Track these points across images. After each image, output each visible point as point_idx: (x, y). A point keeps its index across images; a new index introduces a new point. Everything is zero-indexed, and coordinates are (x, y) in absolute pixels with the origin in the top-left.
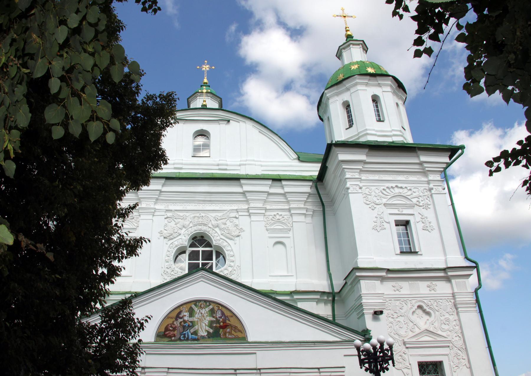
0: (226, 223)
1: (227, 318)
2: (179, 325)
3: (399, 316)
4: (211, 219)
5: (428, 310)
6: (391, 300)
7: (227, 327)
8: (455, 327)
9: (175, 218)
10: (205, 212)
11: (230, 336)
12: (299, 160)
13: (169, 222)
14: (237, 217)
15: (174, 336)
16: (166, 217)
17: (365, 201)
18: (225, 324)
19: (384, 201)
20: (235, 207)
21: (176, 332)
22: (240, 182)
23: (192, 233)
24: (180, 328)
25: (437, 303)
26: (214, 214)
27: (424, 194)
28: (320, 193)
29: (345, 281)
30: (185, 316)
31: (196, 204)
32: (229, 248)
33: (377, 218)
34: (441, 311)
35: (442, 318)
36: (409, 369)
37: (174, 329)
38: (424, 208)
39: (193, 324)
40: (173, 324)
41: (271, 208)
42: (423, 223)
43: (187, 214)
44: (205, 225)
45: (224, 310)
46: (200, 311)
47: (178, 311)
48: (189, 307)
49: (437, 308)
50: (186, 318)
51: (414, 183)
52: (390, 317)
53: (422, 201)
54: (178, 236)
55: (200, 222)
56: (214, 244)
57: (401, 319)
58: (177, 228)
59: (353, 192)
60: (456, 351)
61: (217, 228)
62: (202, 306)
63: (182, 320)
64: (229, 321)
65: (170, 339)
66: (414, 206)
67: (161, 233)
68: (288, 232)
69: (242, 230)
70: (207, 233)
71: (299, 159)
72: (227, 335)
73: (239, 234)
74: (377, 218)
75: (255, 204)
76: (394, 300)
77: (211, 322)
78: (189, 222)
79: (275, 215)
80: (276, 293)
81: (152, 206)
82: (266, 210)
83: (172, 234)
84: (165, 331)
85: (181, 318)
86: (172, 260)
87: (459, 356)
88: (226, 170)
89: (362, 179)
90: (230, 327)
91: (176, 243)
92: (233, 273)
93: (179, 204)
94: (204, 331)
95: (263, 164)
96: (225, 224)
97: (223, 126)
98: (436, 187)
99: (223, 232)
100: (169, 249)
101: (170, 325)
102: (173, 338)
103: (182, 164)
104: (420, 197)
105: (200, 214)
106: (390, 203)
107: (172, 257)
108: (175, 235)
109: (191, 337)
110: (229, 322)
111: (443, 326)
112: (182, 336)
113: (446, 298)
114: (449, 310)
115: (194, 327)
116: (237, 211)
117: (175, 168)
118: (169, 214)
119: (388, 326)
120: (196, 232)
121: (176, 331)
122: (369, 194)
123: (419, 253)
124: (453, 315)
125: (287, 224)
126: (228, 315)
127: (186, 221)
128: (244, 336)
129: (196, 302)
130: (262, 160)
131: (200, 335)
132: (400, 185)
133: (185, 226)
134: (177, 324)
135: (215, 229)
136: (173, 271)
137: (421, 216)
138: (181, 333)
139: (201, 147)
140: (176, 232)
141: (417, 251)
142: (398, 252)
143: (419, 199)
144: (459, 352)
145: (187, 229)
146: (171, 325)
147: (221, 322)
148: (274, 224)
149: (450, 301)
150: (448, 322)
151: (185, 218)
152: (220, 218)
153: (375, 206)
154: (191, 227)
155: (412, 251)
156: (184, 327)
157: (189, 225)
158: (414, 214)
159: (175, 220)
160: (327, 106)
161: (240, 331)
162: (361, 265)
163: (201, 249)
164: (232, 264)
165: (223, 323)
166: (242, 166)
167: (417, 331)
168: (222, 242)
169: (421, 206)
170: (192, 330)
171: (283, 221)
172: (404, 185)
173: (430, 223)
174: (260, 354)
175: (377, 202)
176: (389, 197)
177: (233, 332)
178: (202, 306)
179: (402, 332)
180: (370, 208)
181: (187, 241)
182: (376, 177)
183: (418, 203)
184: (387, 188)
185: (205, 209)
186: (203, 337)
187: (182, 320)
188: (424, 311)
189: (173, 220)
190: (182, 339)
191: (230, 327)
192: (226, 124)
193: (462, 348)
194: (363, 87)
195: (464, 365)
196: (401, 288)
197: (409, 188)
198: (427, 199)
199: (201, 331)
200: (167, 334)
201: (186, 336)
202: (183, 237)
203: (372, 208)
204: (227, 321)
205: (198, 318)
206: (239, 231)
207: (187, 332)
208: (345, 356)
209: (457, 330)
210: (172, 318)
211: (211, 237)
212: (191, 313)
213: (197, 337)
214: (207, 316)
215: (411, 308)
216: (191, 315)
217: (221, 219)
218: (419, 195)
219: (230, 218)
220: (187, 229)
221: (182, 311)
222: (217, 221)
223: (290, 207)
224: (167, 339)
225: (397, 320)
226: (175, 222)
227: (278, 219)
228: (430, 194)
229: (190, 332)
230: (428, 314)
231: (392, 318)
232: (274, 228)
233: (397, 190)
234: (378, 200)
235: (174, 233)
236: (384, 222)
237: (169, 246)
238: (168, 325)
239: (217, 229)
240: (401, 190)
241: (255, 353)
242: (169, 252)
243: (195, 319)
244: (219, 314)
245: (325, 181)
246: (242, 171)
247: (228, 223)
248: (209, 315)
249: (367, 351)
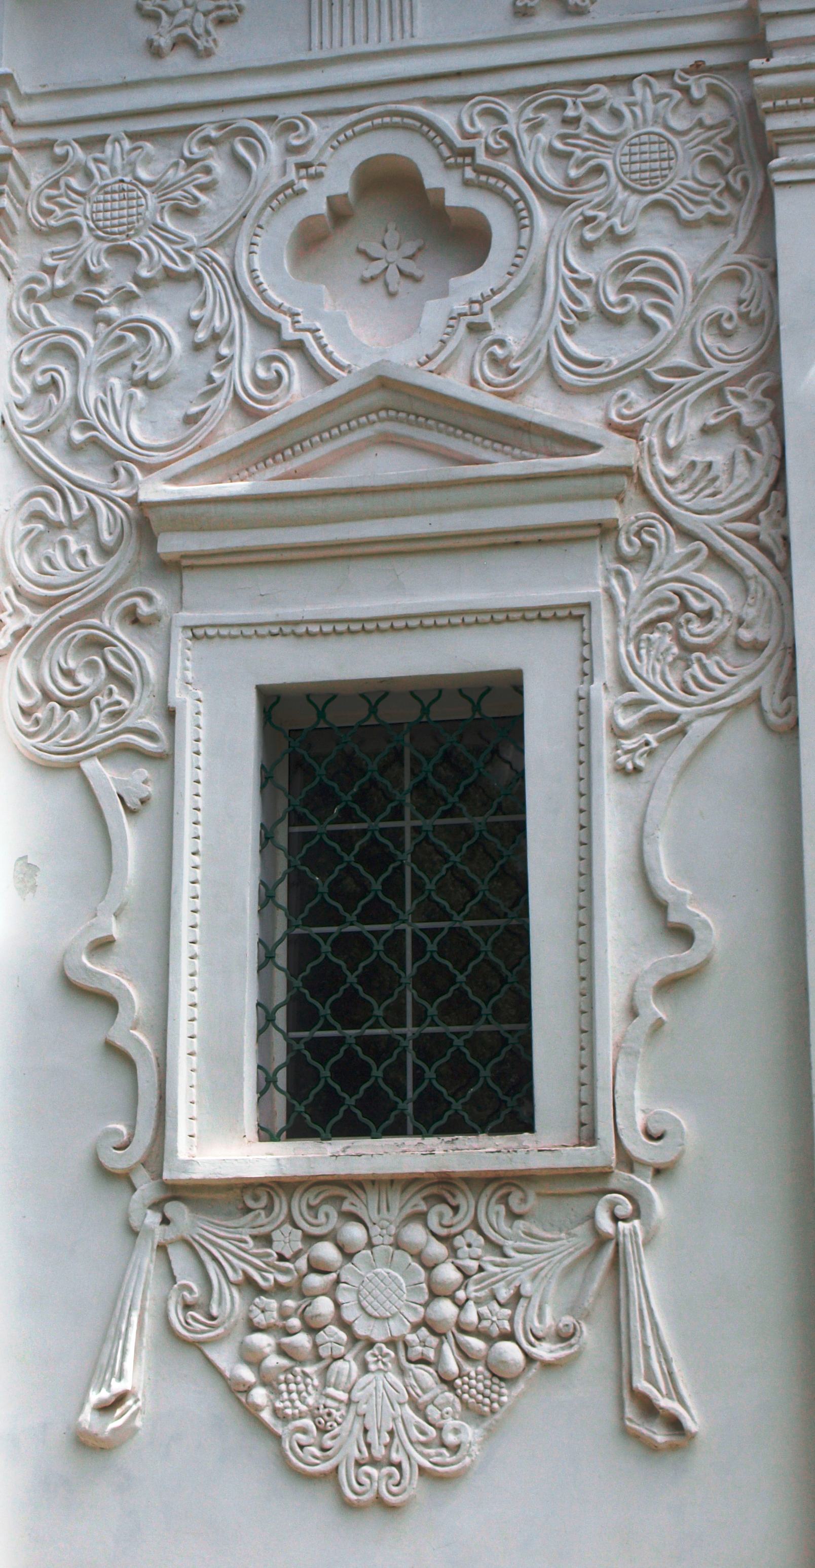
25: (566, 121)
60: (683, 571)
76: (133, 136)
113: (687, 60)
195: (737, 708)
196: (221, 22)
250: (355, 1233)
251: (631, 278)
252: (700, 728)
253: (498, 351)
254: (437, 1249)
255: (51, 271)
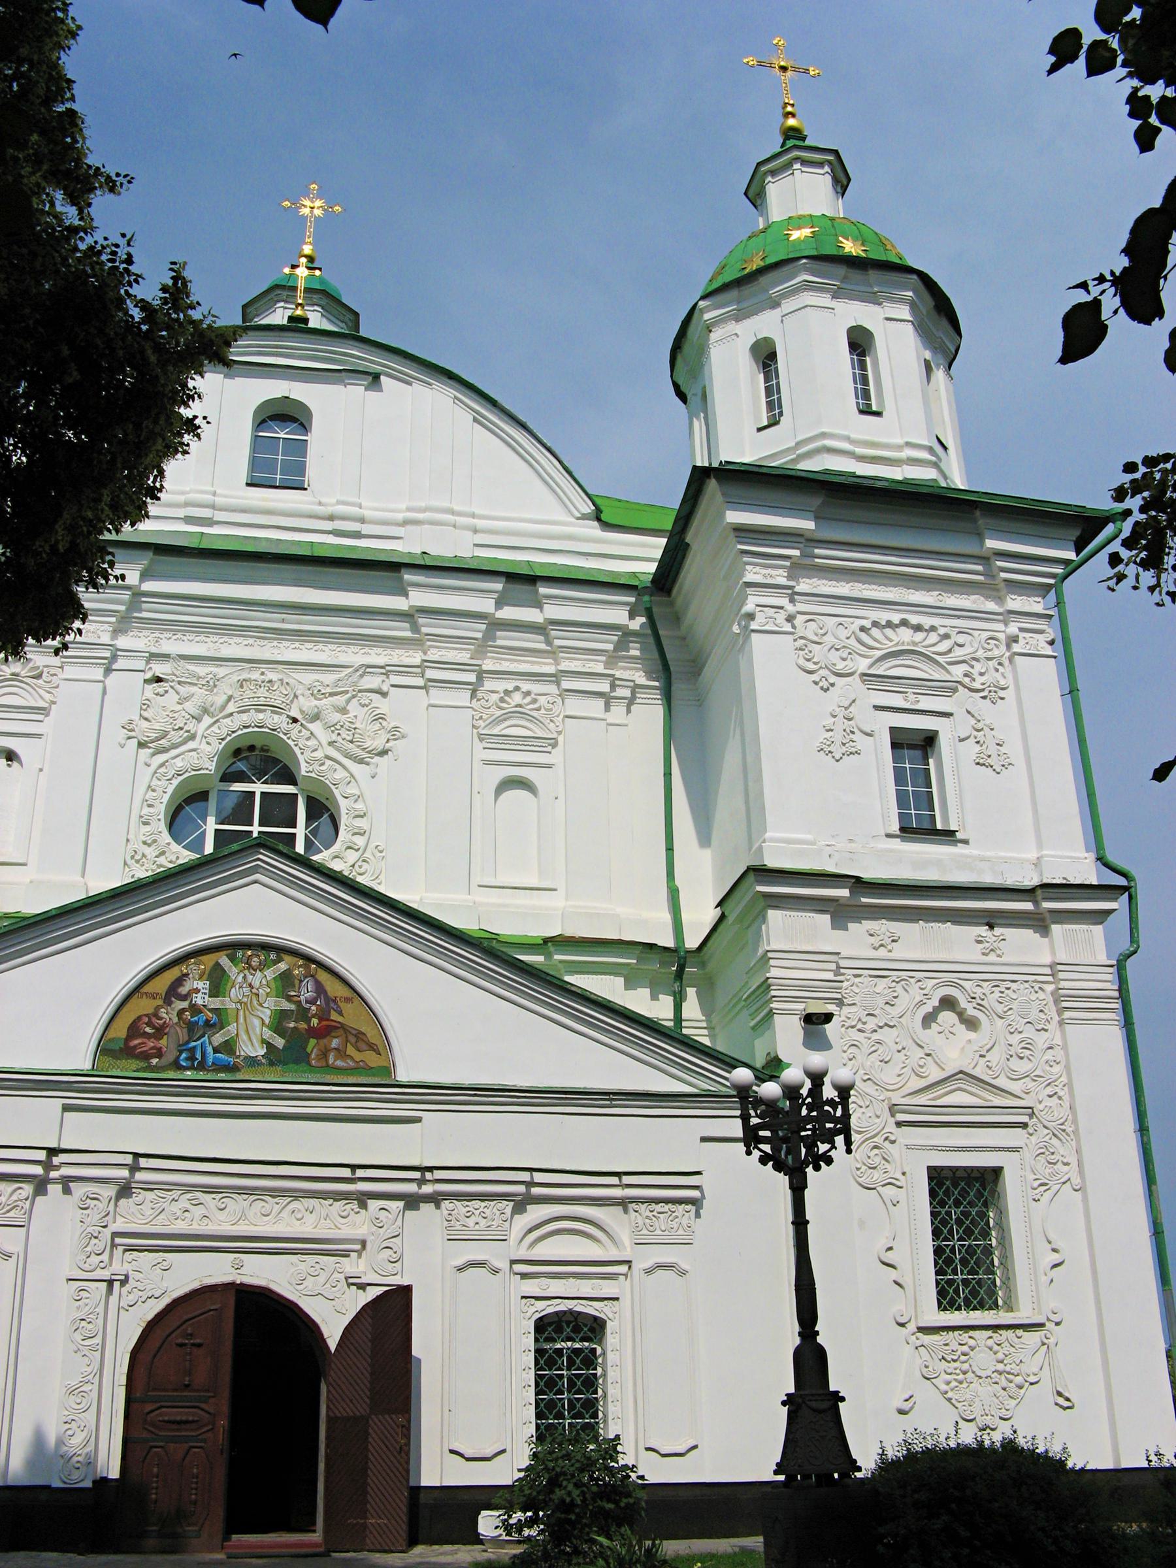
0: (348, 708)
1: (332, 1005)
2: (176, 1020)
3: (881, 1027)
4: (298, 693)
5: (971, 1011)
6: (860, 976)
7: (333, 1034)
8: (1048, 1068)
9: (180, 683)
10: (280, 667)
11: (339, 1063)
12: (598, 519)
13: (157, 694)
14: (385, 688)
15: (159, 1053)
16: (149, 675)
17: (801, 662)
18: (324, 1023)
19: (863, 665)
20: (378, 656)
21: (163, 1042)
22: (401, 579)
23: (234, 735)
24: (177, 1028)
26: (308, 677)
27: (989, 654)
28: (661, 632)
29: (718, 911)
30: (197, 991)
31: (251, 641)
32: (352, 790)
33: (835, 716)
34: (1012, 1017)
35: (1016, 1038)
36: (901, 1187)
37: (160, 1032)
38: (984, 698)
39: (219, 1020)
40: (156, 1015)
41: (498, 668)
42: (978, 742)
43: (221, 671)
44: (276, 709)
45: (323, 976)
46: (245, 977)
47: (174, 973)
48: (214, 962)
49: (1000, 1009)
50: (199, 999)
51: (959, 617)
52: (853, 1027)
53: (982, 674)
54: (184, 742)
55: (262, 701)
56: (303, 773)
57: (886, 1035)
58: (183, 713)
59: (766, 628)
60: (1047, 1139)
61: (318, 722)
62: (255, 962)
63: (185, 1004)
64: (340, 1013)
65: (144, 1064)
66: (955, 690)
67: (128, 727)
68: (549, 749)
69: (396, 734)
70: (281, 735)
71: (598, 516)
72: (331, 1061)
73: (388, 745)
74: (835, 716)
75: (443, 652)
76: (871, 976)
77: (282, 1015)
78: (225, 698)
79: (507, 692)
80: (495, 937)
81: (106, 639)
82: (481, 675)
83: (165, 734)
84: (129, 1037)
85: (184, 998)
86: (162, 816)
87: (1053, 1153)
88: (357, 535)
89: (796, 590)
90: (341, 1032)
91: (179, 763)
92: (362, 871)
93: (192, 636)
94: (257, 1043)
95: (481, 523)
96: (343, 711)
97: (356, 391)
98: (1027, 635)
99: (334, 737)
100: (155, 782)
101: (146, 1020)
102: (155, 1061)
103: (213, 507)
104: (974, 663)
105: (263, 674)
106: (880, 672)
107: (163, 807)
108: (175, 737)
109: (215, 1058)
110: (340, 1019)
111: (1015, 1064)
112: (184, 1055)
114: (1034, 1015)
115: (222, 1028)
116: (386, 670)
117: (189, 520)
118: (159, 669)
119: (845, 1055)
120: (245, 731)
121: (165, 1037)
122: (815, 639)
123: (959, 835)
124: (1046, 1030)
125: (547, 722)
126: (339, 994)
127: (216, 694)
128: (385, 1064)
129: (233, 947)
130: (478, 512)
131: (242, 1053)
132: (914, 619)
133: (212, 709)
134: (169, 1015)
135: (310, 726)
136: (163, 853)
137: (973, 721)
138: (180, 1045)
139: (280, 457)
140: (181, 729)
141: (952, 829)
142: (895, 828)
143: (972, 667)
144: (1055, 1141)
145: (217, 721)
146: (149, 1019)
147: (314, 1016)
148: (505, 720)
149: (1040, 988)
150: (1028, 1052)
151: (211, 683)
152: (329, 690)
153: (833, 679)
154: (231, 714)
155: (939, 827)
156: (191, 1027)
157: (223, 707)
158: (951, 714)
159: (178, 687)
160: (703, 350)
161: (372, 1047)
162: (772, 862)
163: (258, 788)
164: (360, 841)
165: (321, 1019)
166: (409, 528)
167: (935, 1075)
168: (331, 767)
169: (977, 691)
170: (218, 1039)
171: (534, 714)
172: (927, 621)
173: (1001, 746)
174: (433, 1120)
175: (840, 666)
176: (879, 653)
177: (351, 1050)
178: (253, 964)
179: (888, 1076)
180: (816, 683)
181: (215, 759)
182: (844, 588)
183: (967, 680)
184: (875, 624)
185: (280, 658)
186: (252, 1061)
187: (185, 1004)
188: (961, 1015)
189: (172, 687)
190: (184, 1064)
191: (341, 1032)
192: (366, 389)
193: (1064, 1131)
194: (825, 300)
196: (893, 941)
197: (942, 631)
198: (997, 670)
199: (249, 1044)
200: (135, 1047)
201: (199, 1056)
202: (204, 746)
203: (821, 684)
204: (332, 1012)
205: (240, 1002)
206: (389, 736)
207: (199, 1042)
208: (704, 1139)
209: (1054, 1077)
210: (153, 996)
211: (296, 750)
212: (218, 982)
213: (231, 1060)
214: (268, 994)
215: (921, 1003)
216: (215, 992)
217: (331, 695)
218: (973, 656)
219: (360, 691)
220: (217, 721)
221: (187, 975)
222: (320, 699)
223: (560, 668)
224: (134, 1064)
225: (875, 1036)
226: (178, 693)
227: (516, 706)
228: (1007, 654)
229: (210, 1043)
230: (971, 1024)
231: (859, 1030)
232: (504, 732)
233: (905, 636)
234: (844, 660)
235: (174, 730)
236: (855, 730)
237: (155, 772)
238: (139, 1018)
239: (316, 727)
240: (920, 636)
241: (418, 1120)
242: (154, 791)
243: (227, 1003)
244: (306, 992)
245: (679, 592)
246: (407, 545)
247: (353, 707)
248: (274, 993)
249: (770, 1106)
250: (972, 1342)
251: (1023, 1045)
252: (1055, 1188)
253: (990, 1064)
254: (996, 1348)
255: (849, 1018)
